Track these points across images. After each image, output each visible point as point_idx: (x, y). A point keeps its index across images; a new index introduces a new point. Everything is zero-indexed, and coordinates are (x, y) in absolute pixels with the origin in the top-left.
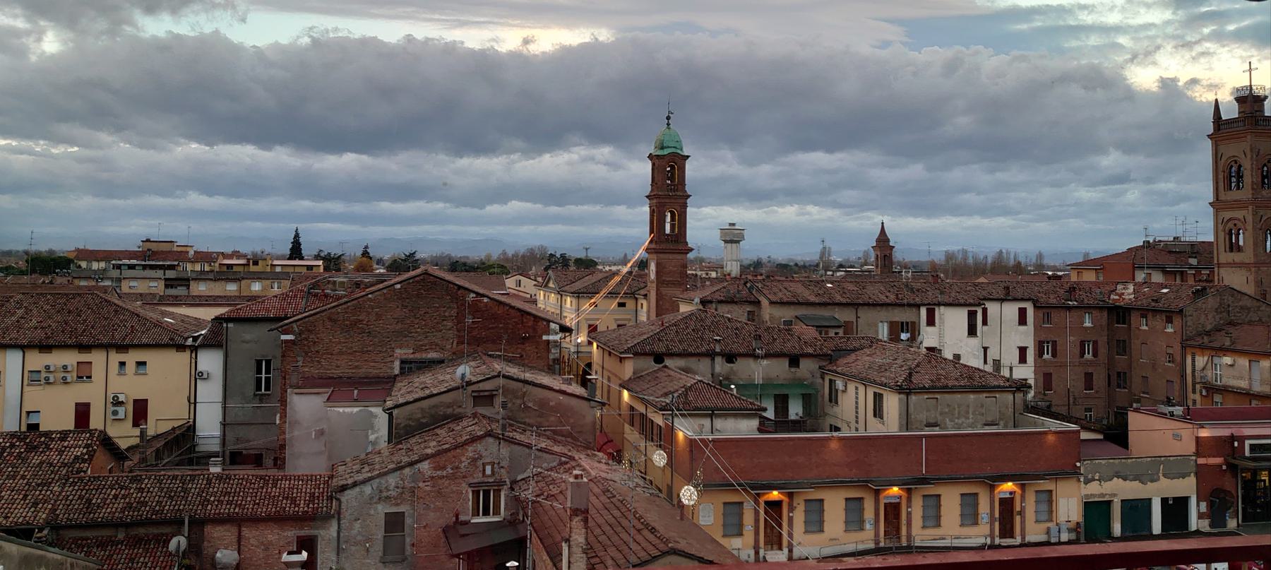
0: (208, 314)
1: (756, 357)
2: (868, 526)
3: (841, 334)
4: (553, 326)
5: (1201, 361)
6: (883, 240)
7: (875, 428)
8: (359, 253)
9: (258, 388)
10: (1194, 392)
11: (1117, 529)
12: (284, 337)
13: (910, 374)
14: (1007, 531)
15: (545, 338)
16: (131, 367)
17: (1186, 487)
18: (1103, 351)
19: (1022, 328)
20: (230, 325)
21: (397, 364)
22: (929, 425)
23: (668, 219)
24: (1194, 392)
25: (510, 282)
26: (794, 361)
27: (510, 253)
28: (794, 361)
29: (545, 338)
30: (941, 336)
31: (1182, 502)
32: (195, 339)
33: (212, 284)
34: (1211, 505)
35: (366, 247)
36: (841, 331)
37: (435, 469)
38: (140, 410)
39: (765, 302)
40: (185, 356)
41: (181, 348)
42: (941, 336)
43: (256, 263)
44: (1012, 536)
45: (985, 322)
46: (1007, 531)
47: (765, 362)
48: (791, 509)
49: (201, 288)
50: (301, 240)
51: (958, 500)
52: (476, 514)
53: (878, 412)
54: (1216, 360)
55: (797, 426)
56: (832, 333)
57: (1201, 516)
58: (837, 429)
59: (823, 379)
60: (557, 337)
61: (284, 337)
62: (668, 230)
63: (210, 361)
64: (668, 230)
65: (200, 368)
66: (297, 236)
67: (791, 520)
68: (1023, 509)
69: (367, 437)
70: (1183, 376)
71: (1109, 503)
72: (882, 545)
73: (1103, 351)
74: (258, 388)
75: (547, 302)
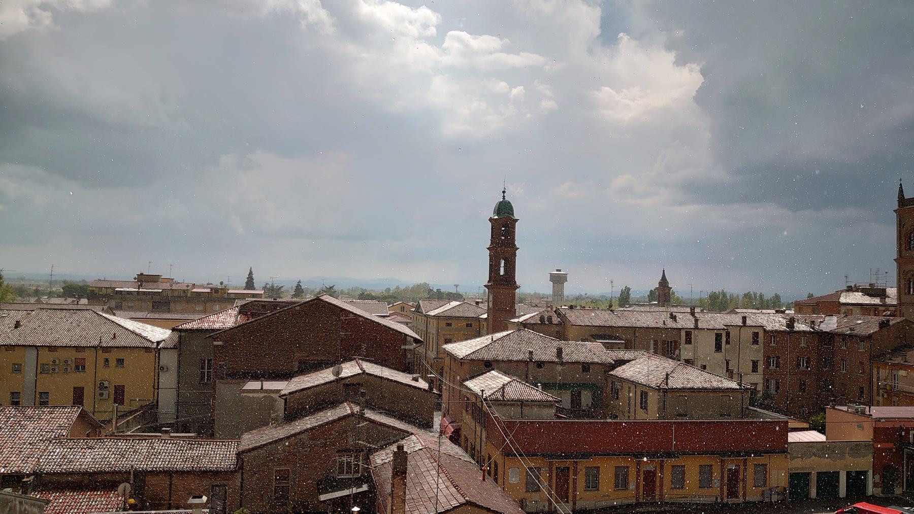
2: (632, 486)
5: (883, 373)
7: (641, 416)
9: (202, 378)
10: (878, 394)
11: (813, 493)
12: (215, 343)
13: (667, 378)
14: (733, 493)
16: (113, 363)
17: (865, 462)
18: (813, 363)
19: (755, 347)
21: (296, 364)
22: (680, 415)
23: (502, 265)
24: (878, 394)
27: (402, 287)
30: (695, 351)
31: (865, 473)
34: (883, 477)
37: (311, 439)
38: (119, 394)
42: (695, 351)
44: (737, 497)
45: (728, 342)
46: (733, 493)
48: (575, 473)
51: (697, 470)
52: (341, 472)
53: (644, 406)
54: (894, 372)
55: (587, 414)
57: (875, 485)
58: (616, 417)
60: (412, 347)
61: (215, 343)
62: (502, 273)
64: (502, 273)
67: (575, 481)
68: (745, 477)
69: (269, 414)
70: (871, 382)
71: (809, 474)
72: (641, 500)
73: (813, 363)
74: (202, 378)
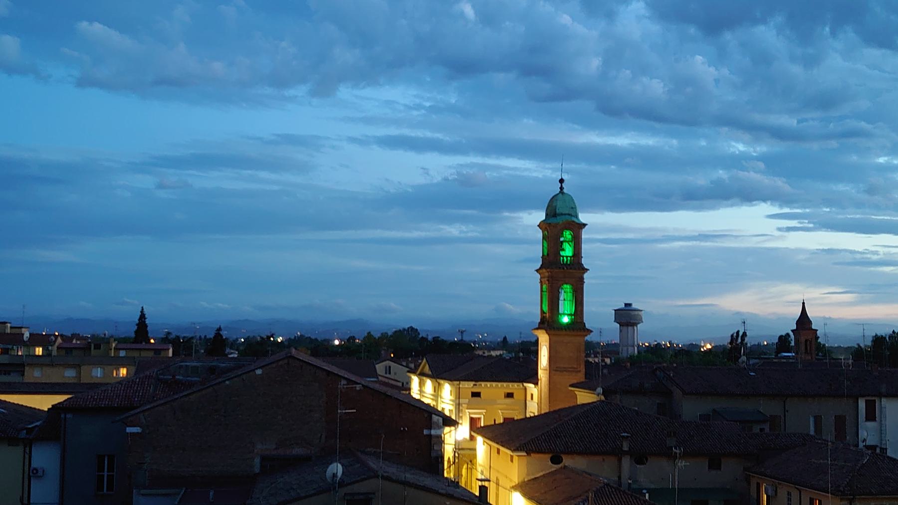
0: (44, 402)
1: (672, 457)
3: (767, 430)
4: (435, 418)
6: (804, 320)
8: (211, 335)
15: (426, 432)
20: (69, 416)
25: (380, 368)
26: (715, 464)
28: (715, 464)
29: (426, 432)
32: (29, 431)
33: (48, 371)
35: (219, 329)
36: (767, 427)
39: (677, 393)
40: (19, 450)
41: (12, 441)
43: (98, 347)
47: (681, 464)
49: (35, 375)
50: (147, 322)
56: (756, 429)
59: (749, 484)
63: (45, 457)
65: (34, 465)
66: (143, 316)
75: (421, 389)
